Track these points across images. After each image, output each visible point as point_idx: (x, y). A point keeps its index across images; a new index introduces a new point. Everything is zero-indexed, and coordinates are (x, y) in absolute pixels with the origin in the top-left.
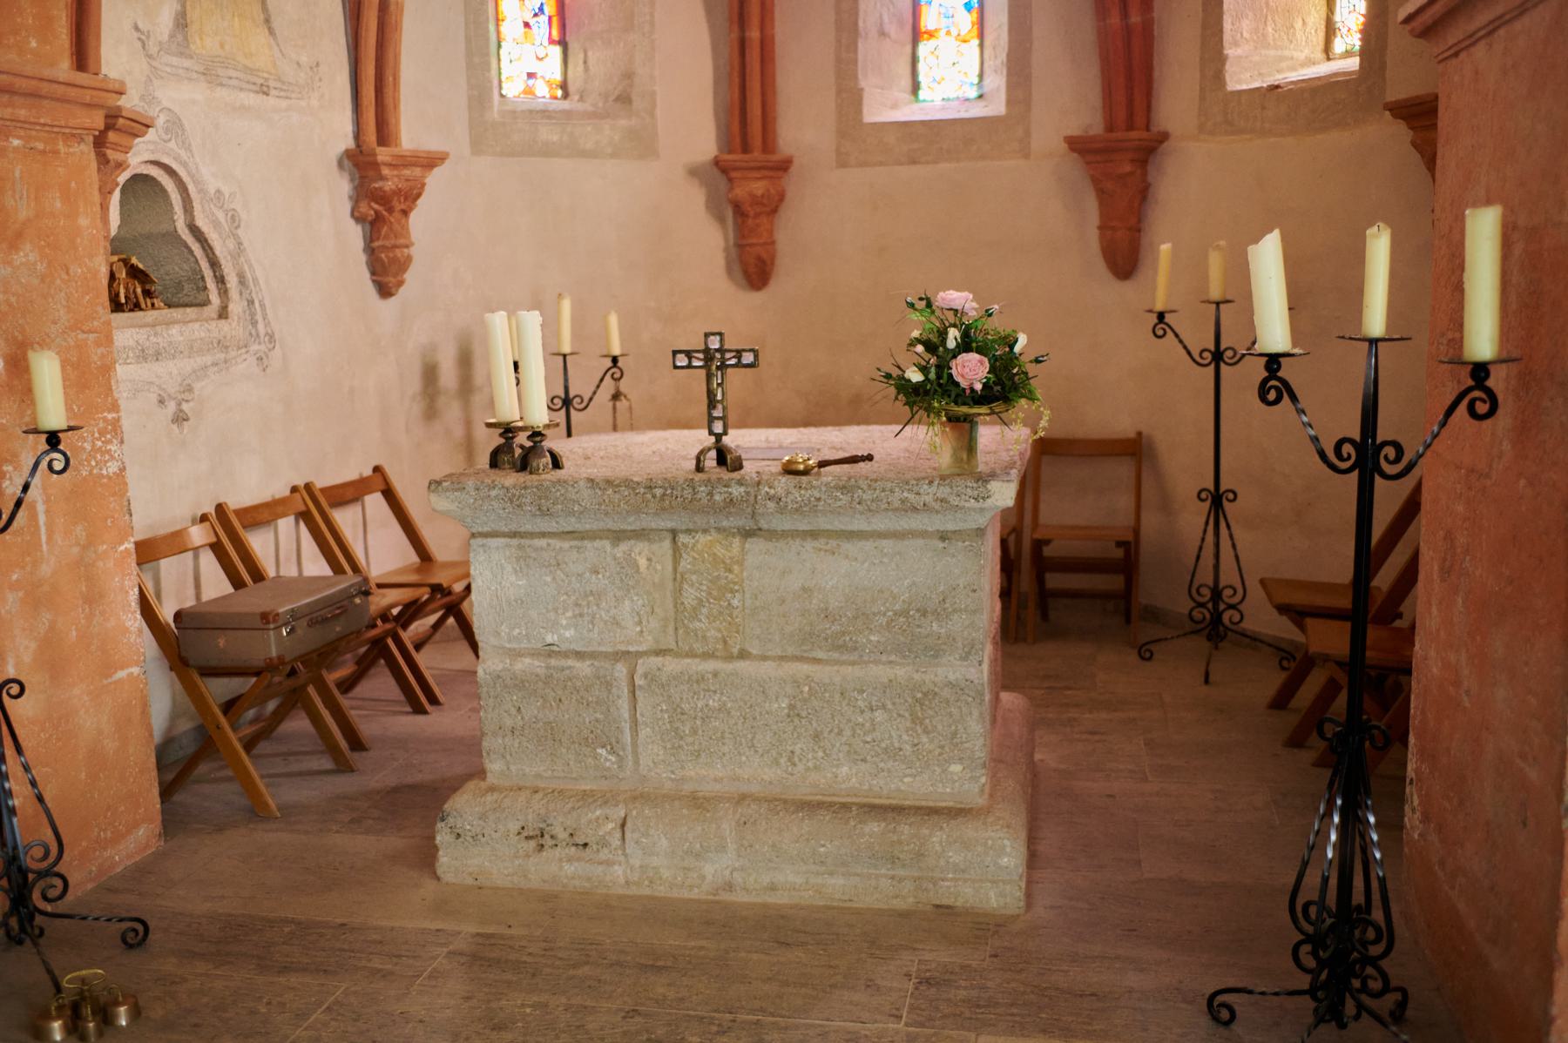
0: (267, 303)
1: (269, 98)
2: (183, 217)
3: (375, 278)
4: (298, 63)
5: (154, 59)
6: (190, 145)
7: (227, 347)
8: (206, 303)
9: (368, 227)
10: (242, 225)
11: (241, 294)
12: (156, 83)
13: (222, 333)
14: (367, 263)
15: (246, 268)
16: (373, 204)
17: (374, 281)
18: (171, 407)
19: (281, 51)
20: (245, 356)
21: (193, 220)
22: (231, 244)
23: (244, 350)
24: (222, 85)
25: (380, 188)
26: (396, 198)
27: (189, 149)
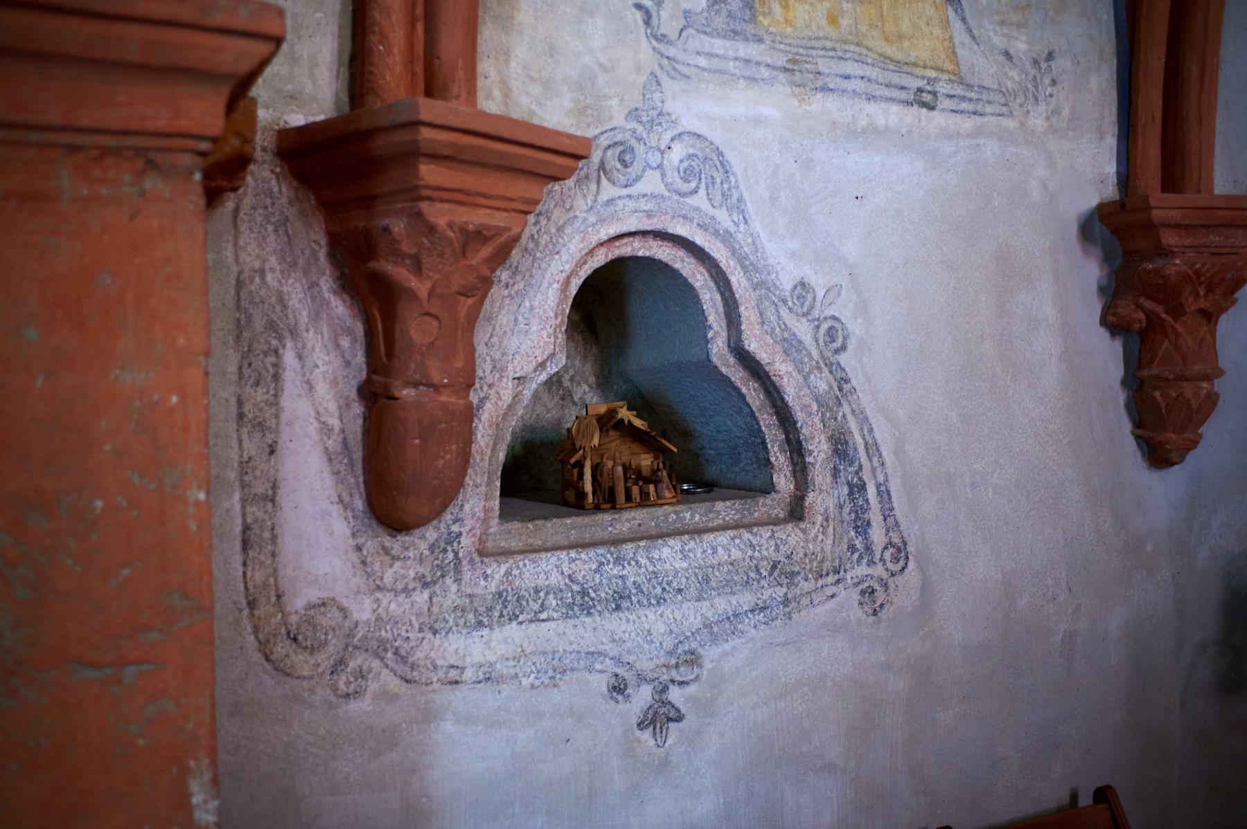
0: (895, 487)
1: (935, 113)
2: (724, 334)
3: (1139, 432)
4: (1007, 54)
5: (670, 43)
6: (740, 200)
7: (793, 575)
8: (768, 489)
9: (1135, 340)
10: (851, 346)
11: (835, 473)
12: (667, 83)
13: (783, 549)
14: (1127, 406)
15: (853, 424)
16: (1142, 300)
17: (1137, 438)
18: (643, 696)
19: (970, 31)
20: (833, 589)
21: (740, 340)
22: (822, 383)
23: (831, 579)
24: (825, 89)
25: (1156, 272)
26: (1188, 289)
27: (739, 206)
